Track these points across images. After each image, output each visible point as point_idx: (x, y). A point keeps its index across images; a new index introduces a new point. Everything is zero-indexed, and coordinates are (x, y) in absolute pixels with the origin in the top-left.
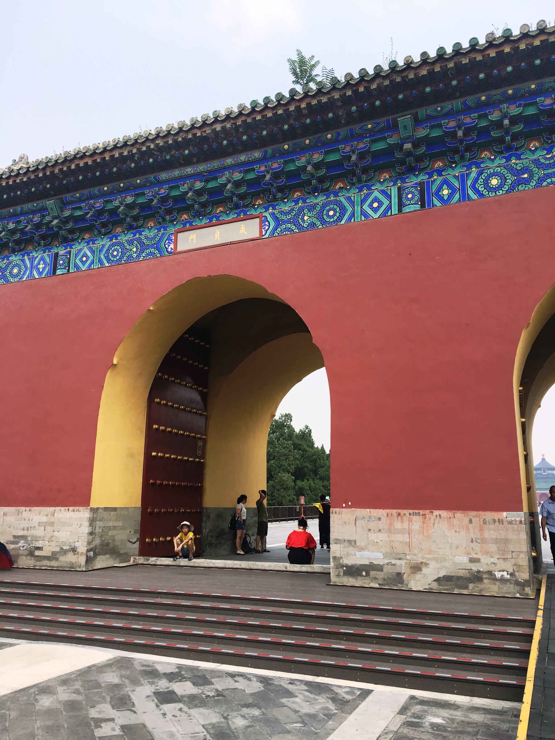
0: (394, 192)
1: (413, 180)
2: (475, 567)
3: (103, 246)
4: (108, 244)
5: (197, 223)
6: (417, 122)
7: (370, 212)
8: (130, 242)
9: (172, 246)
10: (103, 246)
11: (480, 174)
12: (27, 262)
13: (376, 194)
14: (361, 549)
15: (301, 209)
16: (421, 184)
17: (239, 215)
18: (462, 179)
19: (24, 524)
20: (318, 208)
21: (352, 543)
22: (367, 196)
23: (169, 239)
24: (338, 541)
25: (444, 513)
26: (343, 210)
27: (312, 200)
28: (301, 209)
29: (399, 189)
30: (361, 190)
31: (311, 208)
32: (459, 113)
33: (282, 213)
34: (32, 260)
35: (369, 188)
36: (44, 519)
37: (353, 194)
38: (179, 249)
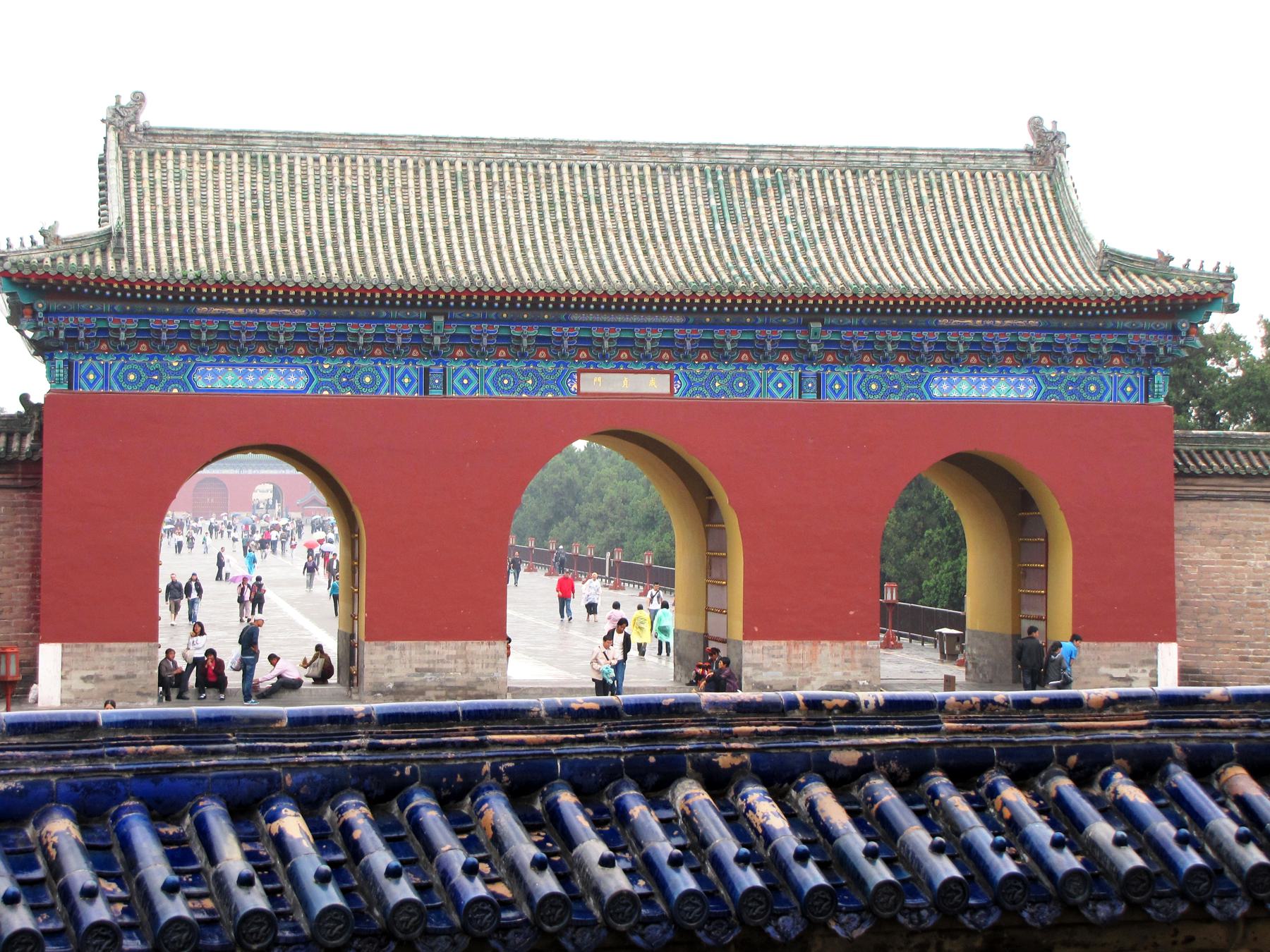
0: (796, 377)
1: (812, 371)
2: (846, 679)
3: (490, 370)
4: (495, 370)
5: (602, 366)
6: (824, 327)
7: (775, 391)
8: (525, 373)
9: (575, 386)
10: (490, 370)
11: (864, 377)
12: (384, 372)
13: (780, 375)
14: (768, 670)
15: (712, 376)
16: (818, 375)
17: (648, 366)
18: (850, 378)
19: (427, 657)
20: (729, 377)
21: (757, 666)
22: (772, 375)
23: (571, 377)
24: (748, 665)
25: (828, 643)
26: (751, 385)
27: (722, 369)
28: (712, 376)
29: (800, 375)
30: (767, 368)
31: (723, 376)
32: (854, 327)
33: (693, 374)
34: (392, 371)
35: (774, 368)
36: (454, 652)
37: (760, 369)
38: (583, 389)
